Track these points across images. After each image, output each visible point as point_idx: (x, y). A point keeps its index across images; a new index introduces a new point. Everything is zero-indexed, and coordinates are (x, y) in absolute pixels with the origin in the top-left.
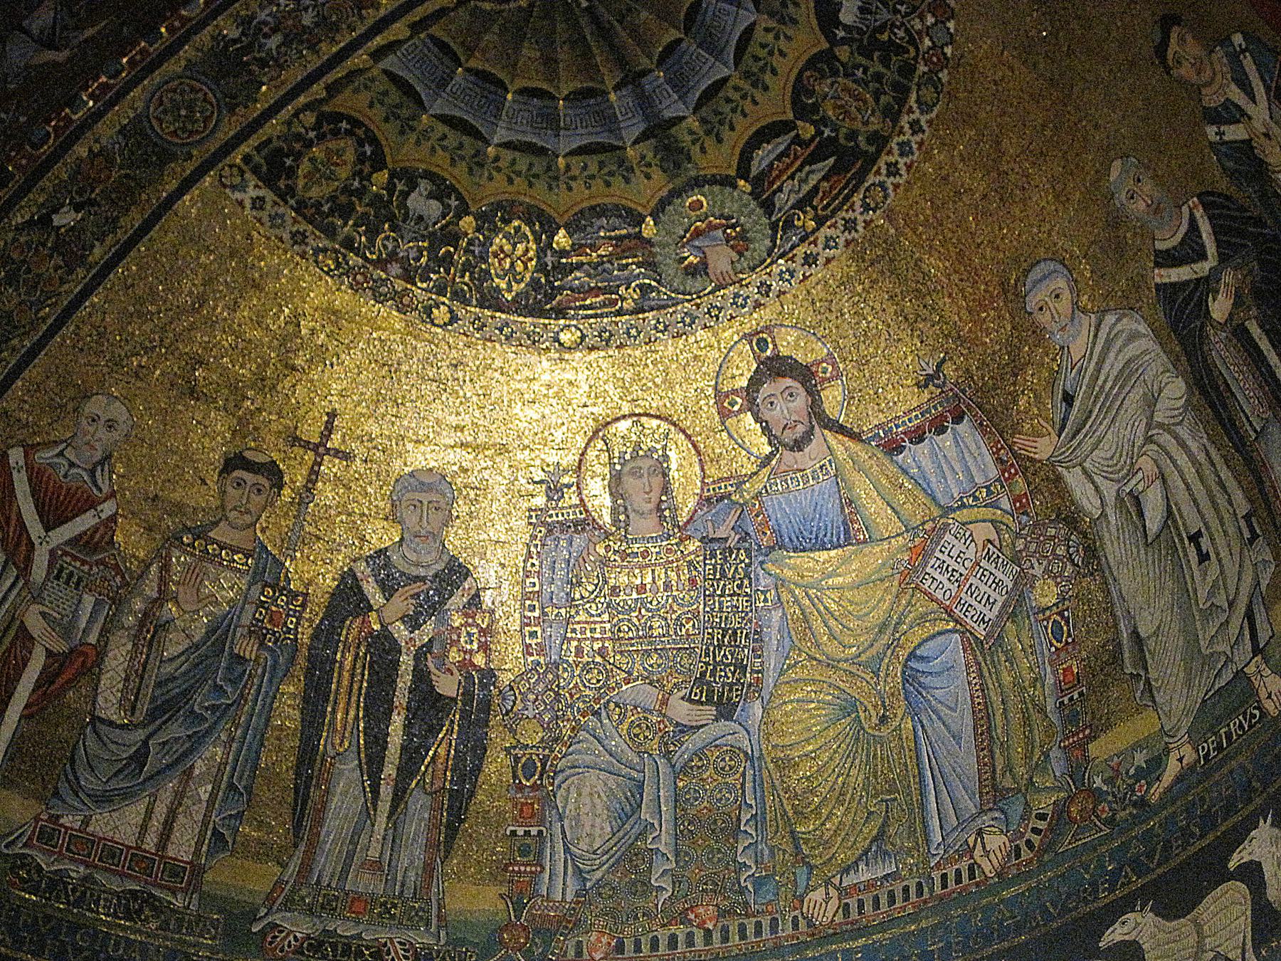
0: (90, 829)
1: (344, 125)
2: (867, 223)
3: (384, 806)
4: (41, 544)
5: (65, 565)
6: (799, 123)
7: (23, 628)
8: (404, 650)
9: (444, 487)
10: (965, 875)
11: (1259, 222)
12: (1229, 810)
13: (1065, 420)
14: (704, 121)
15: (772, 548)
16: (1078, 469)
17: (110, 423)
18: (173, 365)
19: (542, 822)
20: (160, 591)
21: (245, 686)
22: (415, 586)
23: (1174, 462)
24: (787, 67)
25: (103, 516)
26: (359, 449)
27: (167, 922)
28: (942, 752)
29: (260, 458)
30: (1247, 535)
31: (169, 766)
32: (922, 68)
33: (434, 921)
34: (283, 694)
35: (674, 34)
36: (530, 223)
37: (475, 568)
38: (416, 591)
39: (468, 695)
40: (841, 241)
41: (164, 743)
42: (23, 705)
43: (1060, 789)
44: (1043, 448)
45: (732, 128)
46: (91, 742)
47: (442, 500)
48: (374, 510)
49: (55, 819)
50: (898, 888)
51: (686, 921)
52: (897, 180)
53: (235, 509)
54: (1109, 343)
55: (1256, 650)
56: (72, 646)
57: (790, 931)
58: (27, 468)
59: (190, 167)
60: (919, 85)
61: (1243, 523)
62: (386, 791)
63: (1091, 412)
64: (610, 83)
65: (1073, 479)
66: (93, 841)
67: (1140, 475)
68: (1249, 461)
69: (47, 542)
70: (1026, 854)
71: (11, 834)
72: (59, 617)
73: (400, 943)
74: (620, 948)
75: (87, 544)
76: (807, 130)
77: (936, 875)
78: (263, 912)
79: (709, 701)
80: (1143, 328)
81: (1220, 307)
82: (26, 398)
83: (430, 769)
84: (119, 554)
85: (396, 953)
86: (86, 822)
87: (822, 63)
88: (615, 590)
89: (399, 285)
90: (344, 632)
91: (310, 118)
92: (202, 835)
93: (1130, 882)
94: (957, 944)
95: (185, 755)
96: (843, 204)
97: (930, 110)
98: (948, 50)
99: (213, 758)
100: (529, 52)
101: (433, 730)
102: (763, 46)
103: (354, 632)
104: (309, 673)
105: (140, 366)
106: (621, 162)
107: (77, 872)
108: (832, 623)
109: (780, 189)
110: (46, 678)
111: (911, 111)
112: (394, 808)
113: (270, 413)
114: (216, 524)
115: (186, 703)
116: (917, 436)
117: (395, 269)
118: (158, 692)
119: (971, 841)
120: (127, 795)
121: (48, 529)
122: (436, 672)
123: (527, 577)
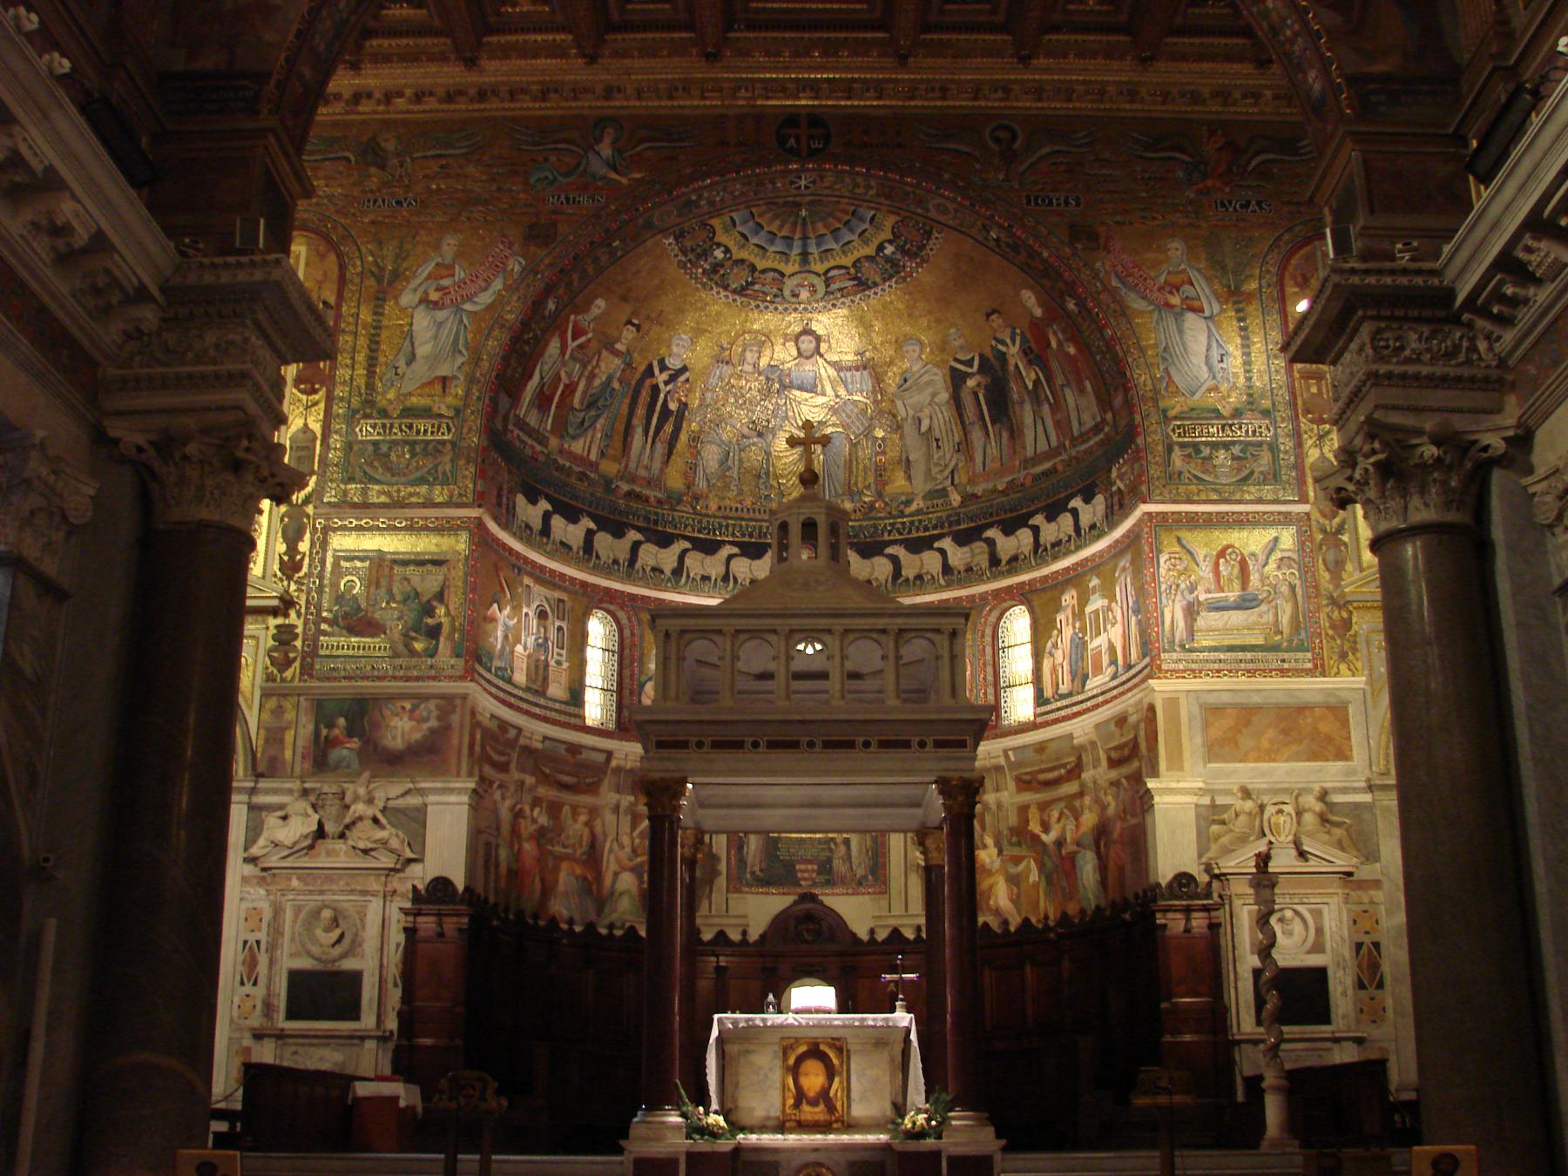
12: (935, 527)
24: (857, 255)
35: (825, 232)
44: (892, 389)
55: (952, 483)
62: (650, 440)
64: (797, 236)
65: (899, 403)
68: (964, 428)
74: (720, 508)
75: (581, 346)
81: (971, 383)
87: (869, 258)
100: (778, 223)
107: (568, 464)
110: (563, 392)
116: (849, 369)
117: (700, 270)
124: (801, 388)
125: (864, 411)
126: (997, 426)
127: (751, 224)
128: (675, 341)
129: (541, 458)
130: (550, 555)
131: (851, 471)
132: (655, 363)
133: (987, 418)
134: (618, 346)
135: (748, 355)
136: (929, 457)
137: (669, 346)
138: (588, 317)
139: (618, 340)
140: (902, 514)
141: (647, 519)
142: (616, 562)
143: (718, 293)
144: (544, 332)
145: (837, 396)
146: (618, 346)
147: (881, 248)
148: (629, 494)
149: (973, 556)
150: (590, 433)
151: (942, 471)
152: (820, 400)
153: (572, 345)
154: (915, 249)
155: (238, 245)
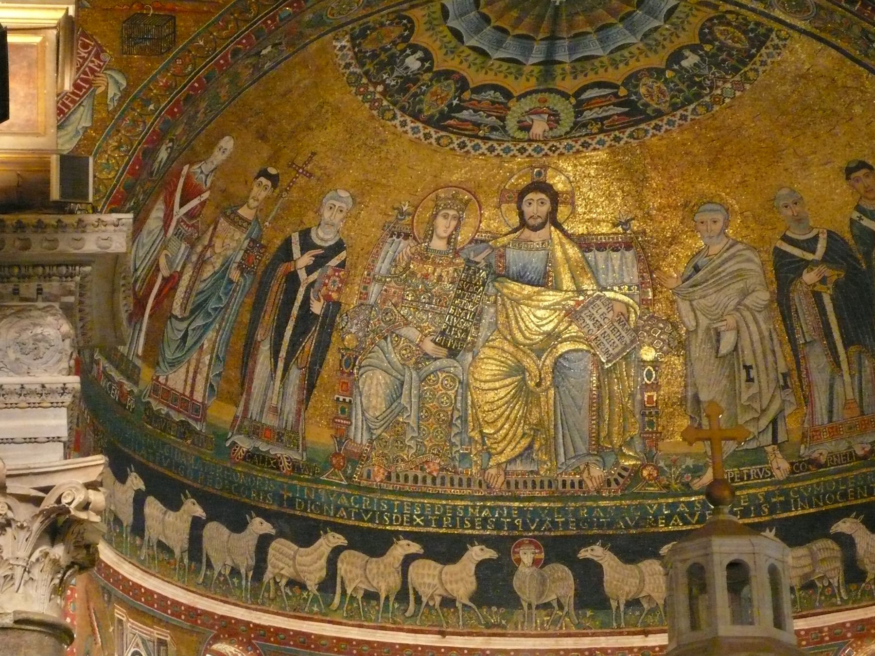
0: (168, 383)
1: (405, 21)
2: (627, 142)
3: (279, 373)
6: (622, 88)
7: (158, 265)
10: (577, 485)
11: (856, 260)
13: (689, 277)
14: (573, 67)
15: (500, 276)
16: (688, 303)
19: (351, 395)
23: (748, 328)
24: (635, 65)
26: (318, 173)
28: (568, 410)
30: (782, 382)
31: (195, 343)
32: (707, 99)
35: (589, 29)
36: (456, 82)
39: (325, 315)
40: (607, 144)
41: (193, 330)
43: (637, 459)
45: (586, 75)
49: (158, 377)
50: (538, 480)
51: (422, 469)
52: (657, 132)
54: (733, 256)
57: (477, 488)
59: (327, 28)
60: (699, 105)
61: (780, 377)
62: (281, 365)
63: (707, 280)
65: (684, 306)
67: (724, 323)
70: (614, 486)
74: (389, 477)
75: (190, 215)
76: (622, 92)
77: (560, 479)
78: (230, 434)
79: (445, 346)
80: (757, 260)
81: (809, 277)
86: (167, 380)
88: (413, 274)
89: (378, 96)
91: (391, 17)
92: (206, 387)
93: (678, 525)
94: (573, 522)
95: (200, 337)
96: (619, 129)
97: (698, 115)
98: (727, 100)
99: (211, 340)
100: (514, 14)
102: (630, 53)
106: (520, 69)
107: (164, 410)
108: (521, 323)
109: (591, 109)
111: (686, 110)
114: (242, 206)
116: (601, 247)
117: (380, 88)
119: (582, 467)
124: (520, 278)
125: (623, 318)
126: (853, 349)
127: (473, 14)
128: (328, 202)
129: (131, 403)
130: (144, 567)
131: (600, 416)
133: (836, 335)
134: (243, 212)
135: (441, 222)
136: (734, 394)
137: (318, 212)
138: (207, 167)
139: (244, 202)
140: (687, 489)
141: (279, 498)
142: (235, 572)
143: (404, 124)
144: (148, 194)
145: (580, 291)
146: (243, 212)
147: (676, 57)
148: (252, 456)
149: (815, 562)
150: (195, 356)
151: (758, 419)
152: (550, 297)
153: (179, 212)
154: (734, 62)
155: (55, 194)
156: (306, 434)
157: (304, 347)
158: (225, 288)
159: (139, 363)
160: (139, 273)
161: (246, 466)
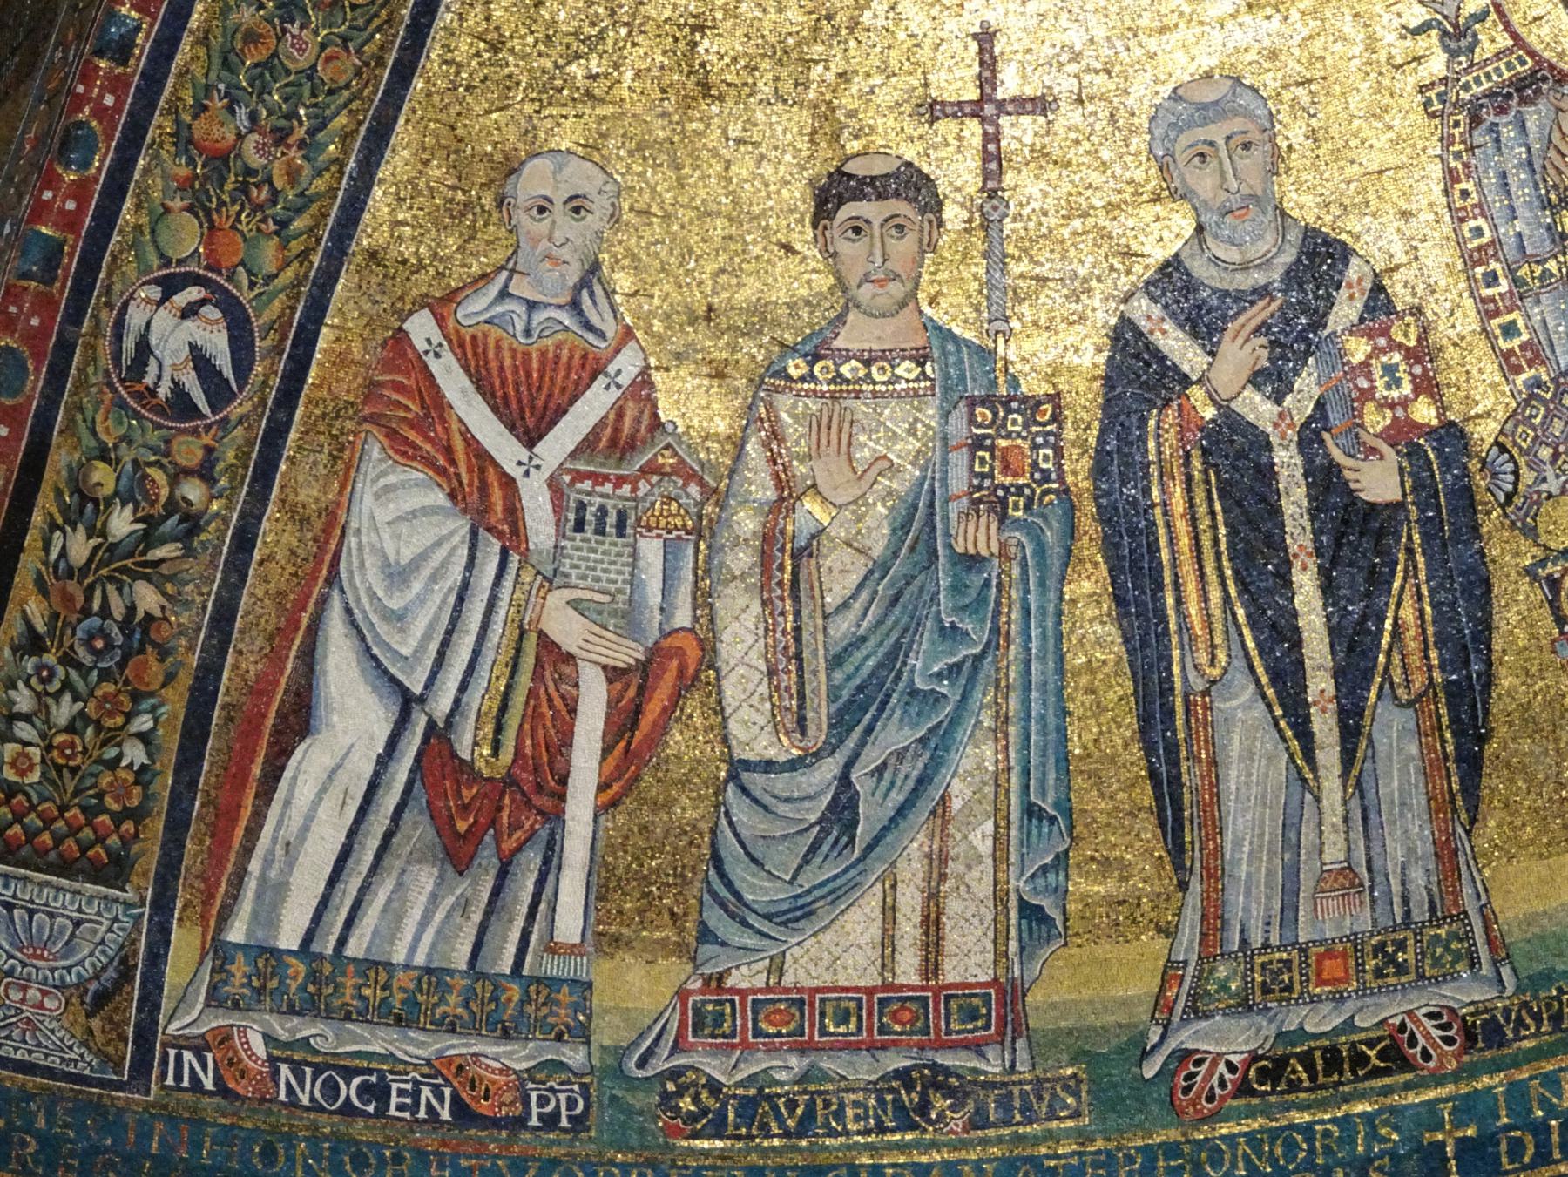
0: (788, 980)
3: (1329, 756)
4: (527, 474)
5: (586, 499)
7: (547, 644)
8: (1274, 440)
9: (1246, 99)
17: (575, 203)
18: (647, 53)
20: (779, 485)
21: (997, 613)
22: (1256, 309)
25: (624, 380)
26: (1065, 85)
27: (981, 1111)
29: (879, 168)
31: (902, 811)
33: (1484, 953)
34: (1074, 601)
37: (1357, 238)
38: (1258, 320)
41: (880, 770)
42: (594, 789)
46: (742, 812)
47: (1251, 127)
48: (1130, 189)
53: (866, 279)
56: (650, 644)
58: (450, 342)
62: (1324, 726)
66: (801, 1001)
69: (538, 467)
71: (641, 1036)
72: (607, 599)
73: (1430, 1016)
82: (401, 217)
83: (1396, 658)
84: (680, 443)
85: (1428, 1036)
86: (777, 966)
90: (1151, 444)
95: (923, 781)
101: (1378, 580)
103: (1171, 436)
104: (1110, 546)
105: (593, 77)
107: (786, 1068)
112: (1348, 758)
113: (868, 75)
114: (841, 319)
115: (898, 677)
118: (838, 676)
120: (839, 893)
121: (530, 439)
122: (1349, 462)
123: (1462, 220)
132: (1143, 310)
150: (914, 849)
156: (1497, 905)
157: (1397, 633)
158: (957, 589)
159: (576, 967)
160: (442, 704)
161: (1267, 1112)
